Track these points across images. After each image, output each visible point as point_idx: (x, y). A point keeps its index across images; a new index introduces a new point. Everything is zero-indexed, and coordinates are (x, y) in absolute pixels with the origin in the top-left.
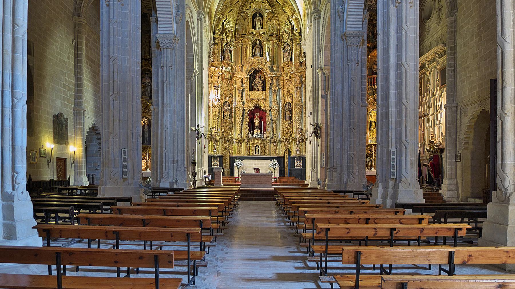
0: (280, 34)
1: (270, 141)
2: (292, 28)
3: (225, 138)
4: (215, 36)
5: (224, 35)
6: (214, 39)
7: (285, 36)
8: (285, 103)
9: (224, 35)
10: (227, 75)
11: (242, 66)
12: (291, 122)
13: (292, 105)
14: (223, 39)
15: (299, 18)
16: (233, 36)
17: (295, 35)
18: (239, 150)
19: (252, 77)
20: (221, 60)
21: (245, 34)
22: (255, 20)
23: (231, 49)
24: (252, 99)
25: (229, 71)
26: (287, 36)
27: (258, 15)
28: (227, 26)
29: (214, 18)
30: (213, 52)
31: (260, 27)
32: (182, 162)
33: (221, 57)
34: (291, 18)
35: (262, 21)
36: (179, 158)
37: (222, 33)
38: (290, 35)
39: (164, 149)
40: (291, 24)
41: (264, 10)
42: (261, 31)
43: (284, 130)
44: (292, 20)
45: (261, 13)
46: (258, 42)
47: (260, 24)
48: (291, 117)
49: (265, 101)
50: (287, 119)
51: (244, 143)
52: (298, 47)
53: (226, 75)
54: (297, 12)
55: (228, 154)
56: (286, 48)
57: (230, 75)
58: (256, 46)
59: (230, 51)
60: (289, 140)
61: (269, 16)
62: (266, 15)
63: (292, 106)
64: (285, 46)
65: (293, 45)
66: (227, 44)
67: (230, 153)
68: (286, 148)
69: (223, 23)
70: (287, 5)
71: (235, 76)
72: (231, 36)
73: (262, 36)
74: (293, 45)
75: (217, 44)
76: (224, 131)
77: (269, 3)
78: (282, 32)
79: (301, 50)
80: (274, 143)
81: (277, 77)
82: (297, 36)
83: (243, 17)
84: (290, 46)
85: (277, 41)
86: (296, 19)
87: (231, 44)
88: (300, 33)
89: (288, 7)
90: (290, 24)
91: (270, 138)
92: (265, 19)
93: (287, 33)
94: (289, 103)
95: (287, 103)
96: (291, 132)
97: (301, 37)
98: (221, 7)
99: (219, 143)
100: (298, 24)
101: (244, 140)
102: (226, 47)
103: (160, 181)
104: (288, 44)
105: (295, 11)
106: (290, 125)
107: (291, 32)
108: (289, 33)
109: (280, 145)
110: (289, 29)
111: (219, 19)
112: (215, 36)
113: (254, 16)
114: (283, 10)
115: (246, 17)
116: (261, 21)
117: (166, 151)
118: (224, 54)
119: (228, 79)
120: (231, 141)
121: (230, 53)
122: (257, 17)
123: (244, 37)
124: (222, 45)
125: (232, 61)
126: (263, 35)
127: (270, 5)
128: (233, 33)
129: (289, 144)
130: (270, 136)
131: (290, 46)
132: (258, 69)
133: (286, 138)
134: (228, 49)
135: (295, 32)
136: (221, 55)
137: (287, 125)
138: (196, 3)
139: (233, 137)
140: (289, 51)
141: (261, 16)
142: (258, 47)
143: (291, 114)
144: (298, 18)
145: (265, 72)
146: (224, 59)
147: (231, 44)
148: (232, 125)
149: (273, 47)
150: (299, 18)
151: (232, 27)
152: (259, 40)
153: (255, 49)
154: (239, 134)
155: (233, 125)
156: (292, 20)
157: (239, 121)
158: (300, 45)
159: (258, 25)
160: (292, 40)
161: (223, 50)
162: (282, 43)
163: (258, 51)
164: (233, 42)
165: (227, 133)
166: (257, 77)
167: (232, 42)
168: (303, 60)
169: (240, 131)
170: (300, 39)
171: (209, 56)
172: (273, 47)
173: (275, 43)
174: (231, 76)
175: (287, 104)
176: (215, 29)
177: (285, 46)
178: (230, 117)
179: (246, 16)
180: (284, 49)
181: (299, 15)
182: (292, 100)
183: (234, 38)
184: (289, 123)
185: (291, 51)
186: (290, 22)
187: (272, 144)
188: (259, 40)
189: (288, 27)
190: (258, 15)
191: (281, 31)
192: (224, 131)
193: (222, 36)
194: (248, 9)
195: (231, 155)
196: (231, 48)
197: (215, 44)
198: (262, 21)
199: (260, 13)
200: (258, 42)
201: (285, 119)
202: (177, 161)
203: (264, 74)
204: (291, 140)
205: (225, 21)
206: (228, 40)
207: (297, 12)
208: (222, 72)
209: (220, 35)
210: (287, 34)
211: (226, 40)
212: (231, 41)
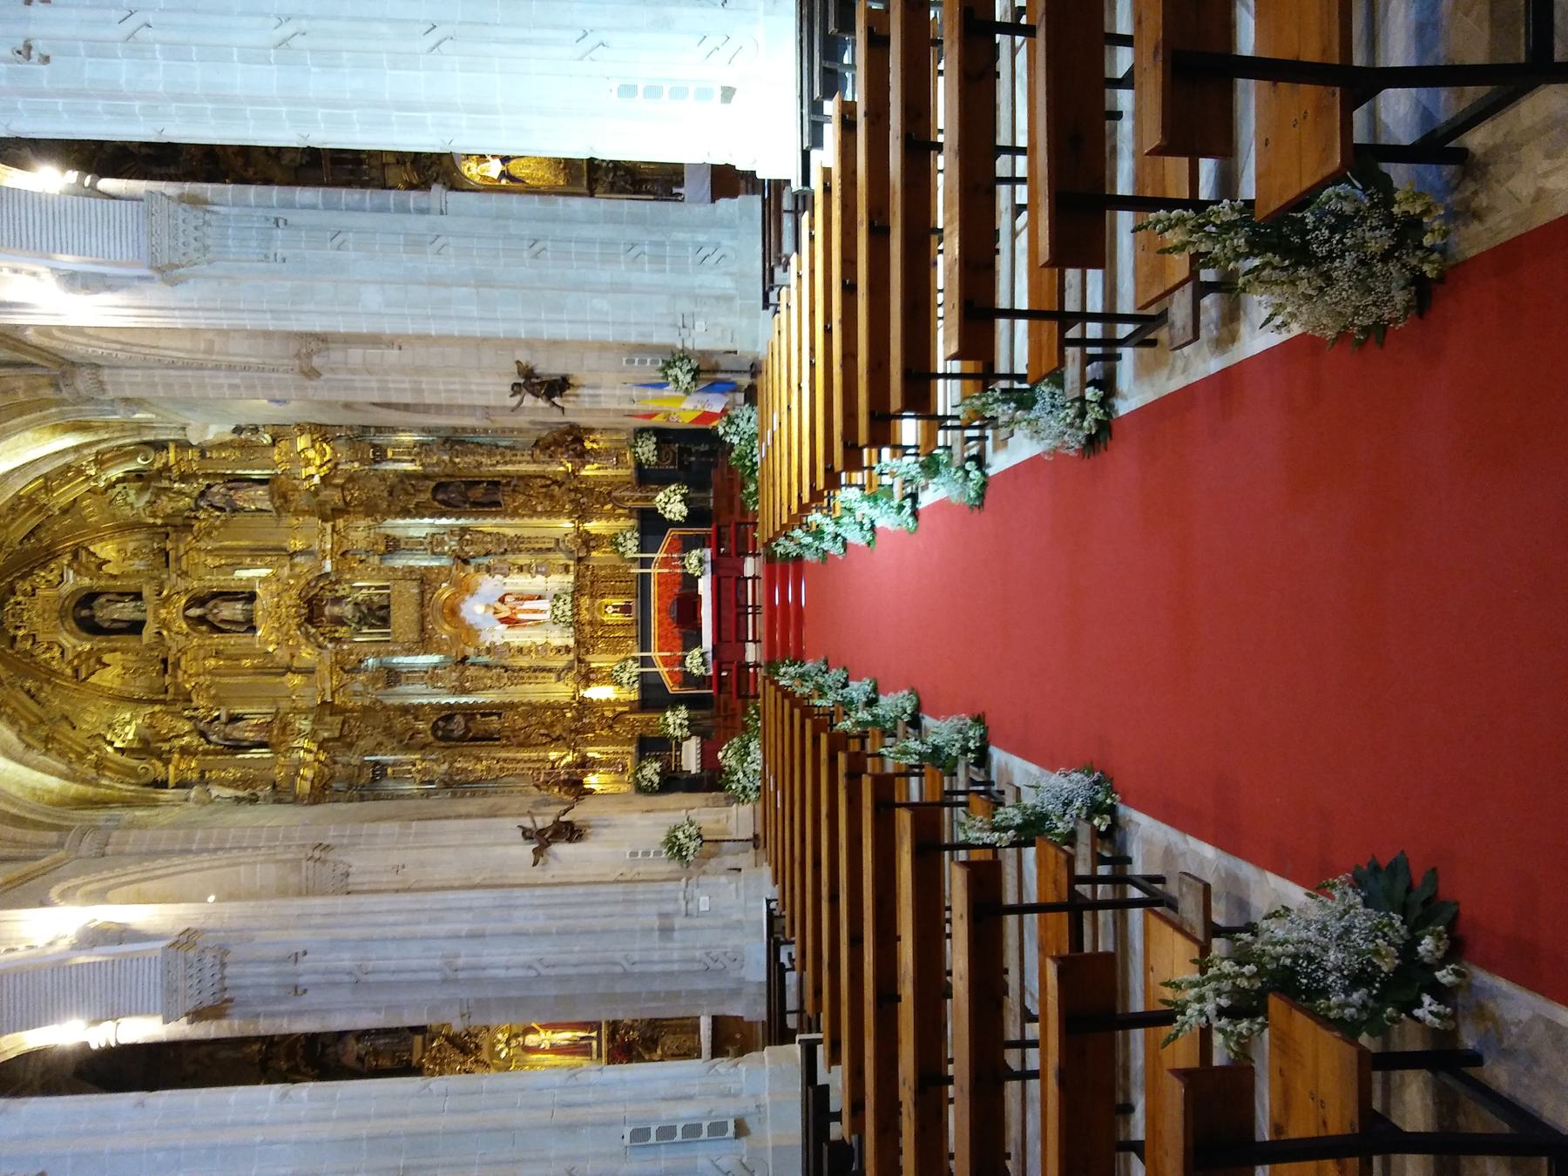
0: (162, 526)
1: (580, 560)
2: (139, 476)
3: (572, 731)
4: (172, 782)
5: (166, 747)
6: (182, 784)
7: (166, 505)
8: (436, 503)
9: (166, 747)
10: (327, 730)
11: (294, 673)
12: (508, 484)
13: (443, 480)
15: (94, 450)
16: (172, 708)
17: (166, 464)
18: (612, 679)
19: (336, 631)
20: (264, 753)
21: (165, 661)
22: (106, 625)
23: (224, 718)
24: (423, 630)
25: (314, 722)
27: (85, 613)
28: (130, 736)
29: (98, 785)
30: (237, 788)
31: (133, 604)
32: (664, 896)
33: (256, 754)
34: (95, 481)
35: (111, 597)
36: (654, 909)
37: (159, 755)
38: (165, 483)
39: (618, 969)
40: (119, 480)
41: (67, 588)
43: (539, 508)
44: (104, 478)
45: (78, 597)
46: (195, 612)
48: (489, 483)
49: (432, 581)
50: (499, 497)
51: (588, 658)
52: (215, 455)
53: (326, 735)
55: (631, 717)
56: (220, 503)
57: (328, 719)
58: (210, 617)
59: (234, 719)
60: (576, 490)
61: (88, 569)
62: (86, 581)
63: (448, 480)
64: (212, 506)
66: (203, 734)
67: (627, 709)
69: (117, 750)
70: (43, 498)
71: (333, 697)
72: (168, 718)
73: (169, 597)
74: (206, 476)
75: (202, 774)
76: (547, 735)
77: (34, 568)
78: (154, 516)
80: (588, 547)
81: (336, 537)
83: (93, 673)
84: (209, 486)
85: (190, 538)
86: (100, 462)
87: (205, 718)
88: (160, 446)
89: (53, 491)
90: (119, 487)
91: (571, 563)
92: (103, 583)
93: (157, 496)
94: (436, 490)
95: (434, 499)
96: (549, 482)
97: (172, 441)
99: (590, 755)
100: (123, 454)
101: (580, 661)
102: (214, 738)
103: (741, 981)
104: (202, 494)
105: (68, 467)
106: (521, 489)
107: (153, 484)
109: (595, 526)
110: (140, 491)
111: (100, 765)
113: (91, 627)
114: (65, 511)
115: (93, 661)
117: (623, 962)
118: (245, 744)
119: (343, 725)
120: (585, 706)
122: (93, 616)
123: (177, 665)
124: (206, 753)
126: (165, 593)
127: (44, 566)
128: (157, 708)
129: (592, 490)
130: (562, 562)
131: (209, 486)
132: (303, 611)
133: (571, 501)
134: (222, 727)
135: (152, 464)
136: (248, 756)
137: (521, 499)
139: (567, 700)
140: (230, 489)
141: (88, 598)
143: (479, 483)
144: (98, 453)
148: (523, 704)
150: (94, 450)
151: (133, 717)
152: (186, 608)
153: (223, 621)
154: (559, 679)
155: (525, 701)
156: (104, 478)
157: (506, 680)
159: (125, 611)
160: (184, 478)
161: (229, 747)
162: (196, 518)
164: (196, 709)
165: (552, 725)
166: (336, 610)
168: (267, 436)
169: (544, 674)
171: (253, 800)
174: (331, 715)
175: (440, 497)
177: (212, 506)
178: (492, 714)
179: (88, 659)
181: (86, 452)
182: (425, 477)
183: (179, 707)
184: (514, 491)
185: (229, 481)
186: (112, 485)
187: (594, 554)
189: (132, 492)
190: (85, 613)
191: (151, 521)
192: (547, 735)
193: (170, 752)
194: (62, 653)
195: (636, 704)
196: (218, 718)
197: (203, 780)
198: (111, 597)
199: (75, 607)
200: (195, 612)
201: (498, 504)
202: (662, 915)
203: (322, 588)
204: (576, 483)
205: (111, 743)
206: (187, 728)
207: (70, 458)
208: (315, 749)
211: (186, 739)
212: (190, 718)
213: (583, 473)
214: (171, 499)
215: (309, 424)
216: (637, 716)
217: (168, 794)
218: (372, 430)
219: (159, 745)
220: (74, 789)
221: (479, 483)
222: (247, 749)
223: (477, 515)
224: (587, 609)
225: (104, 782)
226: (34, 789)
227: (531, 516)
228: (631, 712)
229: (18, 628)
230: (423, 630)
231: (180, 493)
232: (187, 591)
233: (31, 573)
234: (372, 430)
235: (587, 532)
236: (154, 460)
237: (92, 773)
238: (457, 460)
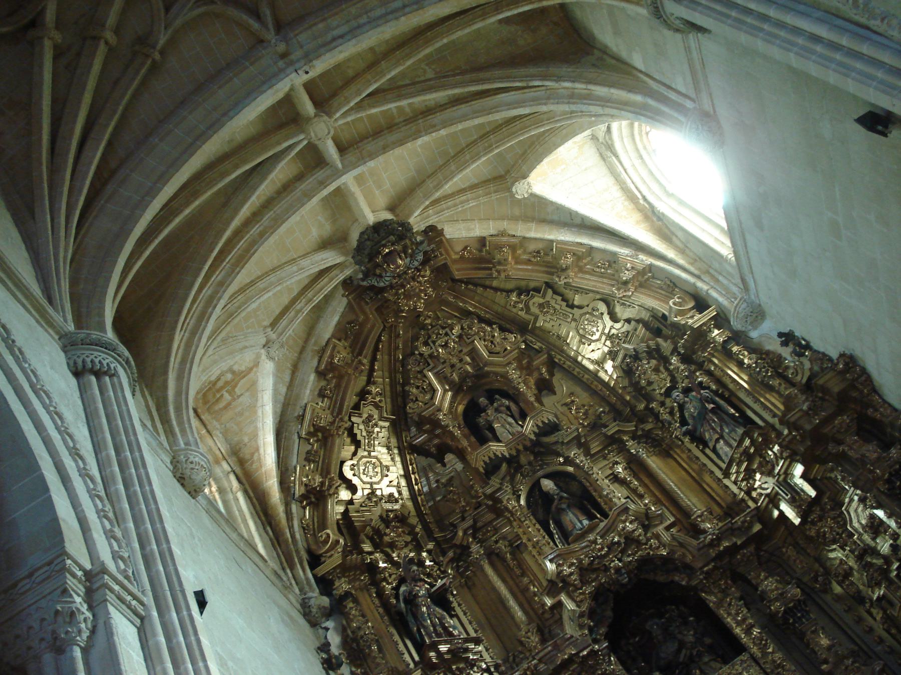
4: (322, 570)
5: (367, 547)
6: (325, 584)
9: (367, 547)
14: (372, 568)
15: (650, 260)
26: (656, 370)
27: (483, 400)
29: (287, 505)
38: (666, 346)
46: (548, 485)
47: (510, 420)
54: (623, 251)
59: (440, 599)
62: (514, 374)
75: (347, 594)
79: (753, 350)
88: (701, 305)
98: (297, 450)
105: (613, 260)
108: (658, 349)
112: (322, 570)
116: (508, 408)
121: (446, 606)
124: (380, 594)
125: (473, 634)
127: (502, 329)
128: (414, 520)
136: (397, 638)
138: (44, 302)
142: (564, 506)
145: (676, 569)
146: (420, 647)
147: (429, 575)
149: (636, 465)
150: (650, 260)
158: (737, 337)
163: (575, 520)
167: (428, 563)
170: (720, 320)
172: (636, 465)
173: (630, 443)
176: (314, 547)
180: (684, 422)
181: (642, 257)
185: (722, 397)
188: (548, 476)
190: (483, 400)
193: (361, 552)
198: (513, 407)
200: (548, 485)
209: (345, 553)
210: (654, 362)
214: (656, 370)
217: (306, 574)
219: (368, 541)
220: (272, 485)
222: (405, 631)
225: (294, 508)
226: (257, 449)
229: (426, 344)
232: (568, 461)
233: (490, 323)
237: (299, 490)
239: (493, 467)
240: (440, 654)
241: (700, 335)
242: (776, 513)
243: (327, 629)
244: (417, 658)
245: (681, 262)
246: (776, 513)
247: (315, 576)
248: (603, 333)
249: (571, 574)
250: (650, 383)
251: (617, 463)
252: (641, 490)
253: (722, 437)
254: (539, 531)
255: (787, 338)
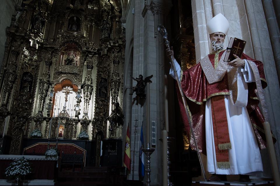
9: (37, 4)
26: (106, 15)
42: (79, 7)
46: (75, 18)
47: (79, 3)
48: (106, 94)
65: (112, 24)
67: (25, 134)
68: (98, 130)
74: (112, 24)
82: (117, 13)
84: (109, 24)
88: (120, 12)
97: (122, 15)
107: (110, 11)
109: (90, 127)
124: (33, 14)
136: (30, 23)
140: (108, 28)
146: (33, 27)
147: (44, 17)
149: (91, 26)
167: (46, 15)
170: (120, 17)
182: (109, 76)
188: (77, 17)
200: (75, 18)
213: (108, 122)
214: (106, 15)
215: (125, 44)
216: (21, 139)
218: (123, 61)
221: (106, 91)
222: (32, 23)
223: (97, 92)
224: (62, 122)
227: (95, 107)
228: (23, 136)
230: (62, 73)
231: (108, 18)
234: (123, 61)
235: (88, 124)
236: (117, 11)
238: (113, 83)
239: (69, 8)
240: (34, 31)
241: (115, 17)
242: (100, 52)
243: (18, 13)
244: (30, 29)
245: (124, 2)
246: (100, 52)
247: (22, 2)
248: (105, 2)
249: (64, 35)
250: (104, 16)
251: (89, 24)
252: (89, 31)
253: (105, 34)
254: (67, 24)
255: (124, 29)
